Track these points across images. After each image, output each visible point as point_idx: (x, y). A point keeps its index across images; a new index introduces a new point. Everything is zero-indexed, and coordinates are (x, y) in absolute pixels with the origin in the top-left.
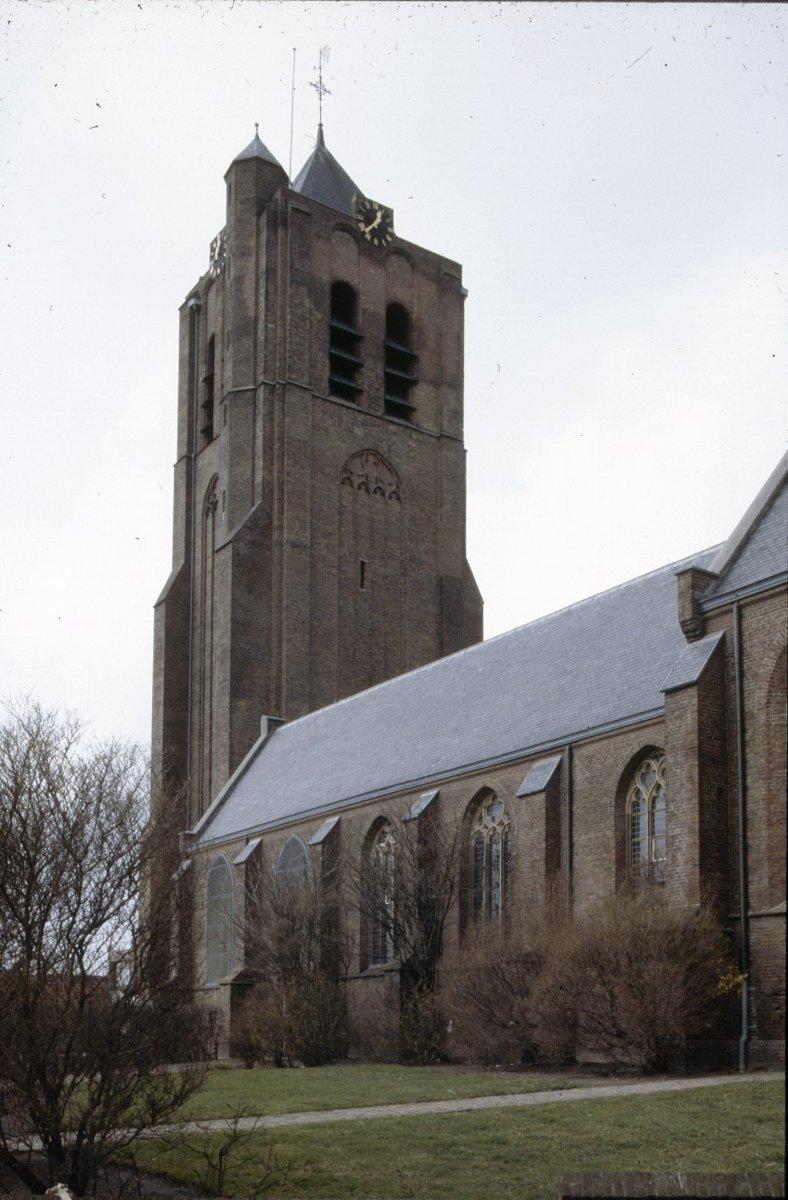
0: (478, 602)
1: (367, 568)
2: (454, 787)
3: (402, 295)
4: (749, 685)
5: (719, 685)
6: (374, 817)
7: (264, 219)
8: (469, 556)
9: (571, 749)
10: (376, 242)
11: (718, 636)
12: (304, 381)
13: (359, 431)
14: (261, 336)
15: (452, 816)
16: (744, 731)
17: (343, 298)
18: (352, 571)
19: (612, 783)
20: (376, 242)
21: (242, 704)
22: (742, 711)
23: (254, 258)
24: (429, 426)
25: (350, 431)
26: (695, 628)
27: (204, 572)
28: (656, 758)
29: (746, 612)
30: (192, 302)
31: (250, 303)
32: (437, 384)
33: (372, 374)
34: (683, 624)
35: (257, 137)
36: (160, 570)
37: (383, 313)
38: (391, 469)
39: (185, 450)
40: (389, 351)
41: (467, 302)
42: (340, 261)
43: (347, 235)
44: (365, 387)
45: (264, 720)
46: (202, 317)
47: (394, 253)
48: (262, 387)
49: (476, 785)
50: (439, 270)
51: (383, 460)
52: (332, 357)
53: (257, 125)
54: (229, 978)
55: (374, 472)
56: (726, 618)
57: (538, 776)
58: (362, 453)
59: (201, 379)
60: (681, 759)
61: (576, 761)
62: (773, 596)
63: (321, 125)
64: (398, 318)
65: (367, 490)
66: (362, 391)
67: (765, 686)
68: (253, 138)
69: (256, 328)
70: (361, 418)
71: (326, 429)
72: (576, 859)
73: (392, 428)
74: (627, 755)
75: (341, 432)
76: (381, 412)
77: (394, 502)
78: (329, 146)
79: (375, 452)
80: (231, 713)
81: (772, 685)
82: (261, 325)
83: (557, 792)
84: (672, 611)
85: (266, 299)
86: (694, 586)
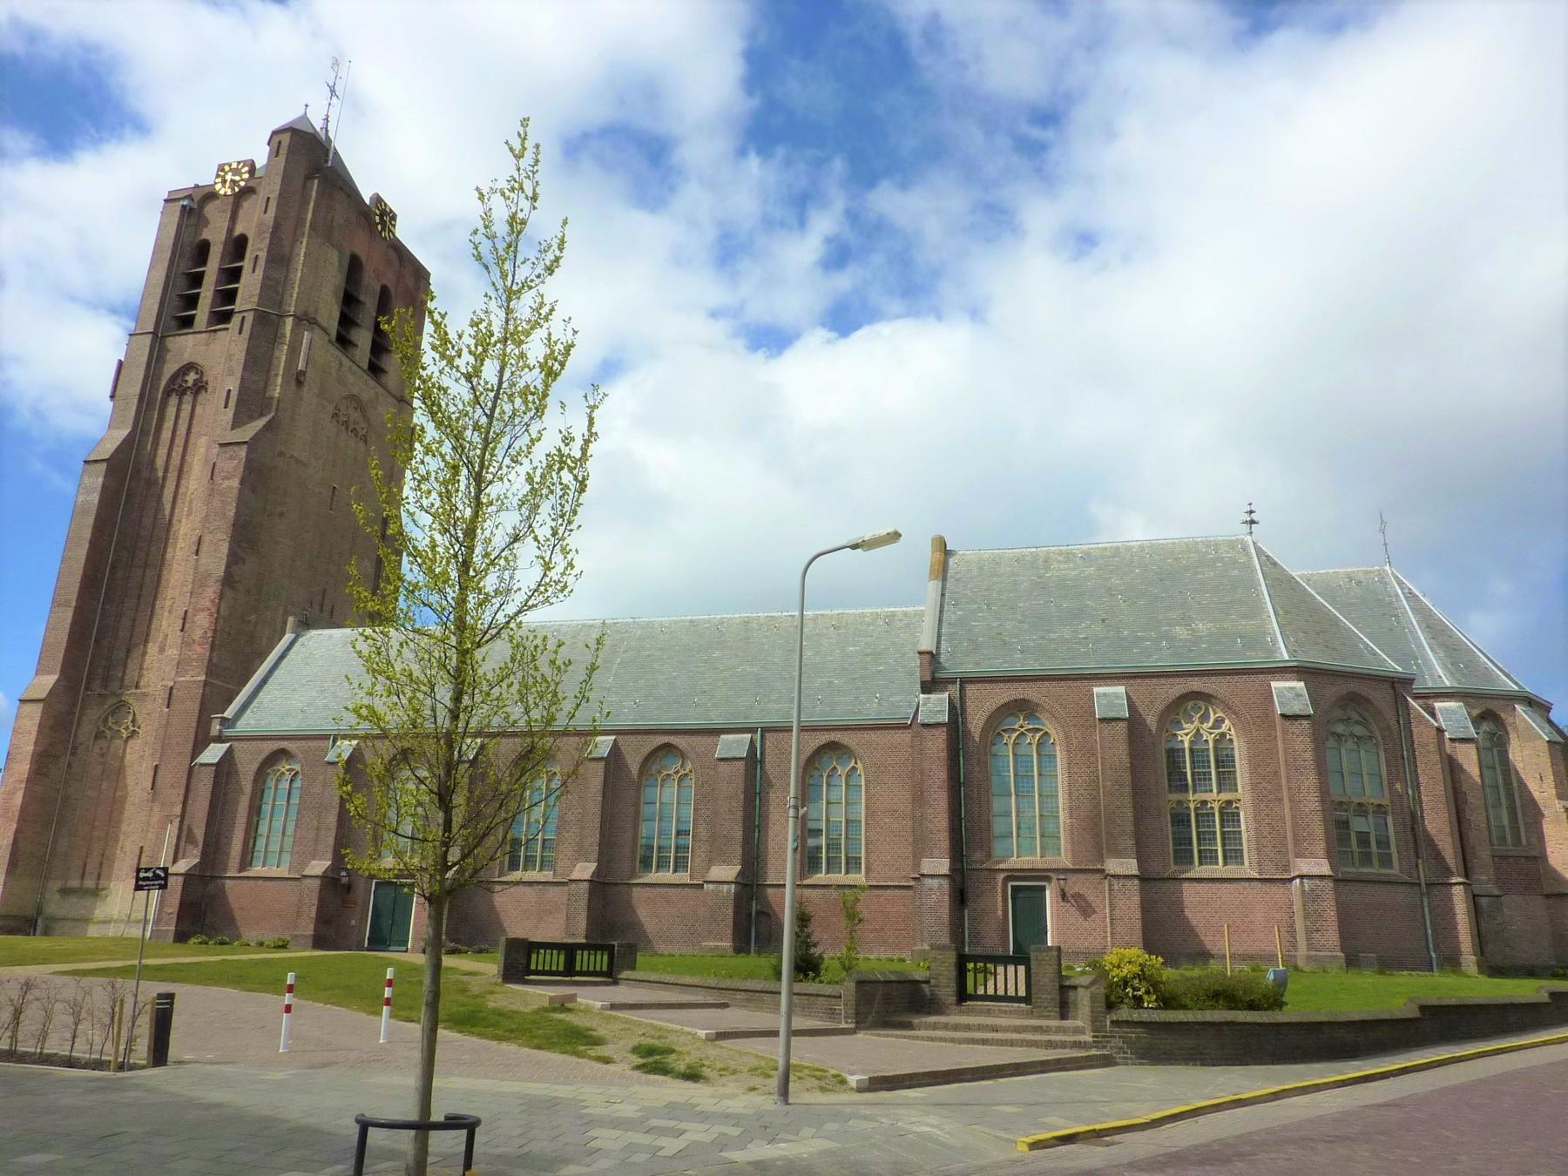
5: (955, 725)
33: (363, 339)
61: (768, 743)
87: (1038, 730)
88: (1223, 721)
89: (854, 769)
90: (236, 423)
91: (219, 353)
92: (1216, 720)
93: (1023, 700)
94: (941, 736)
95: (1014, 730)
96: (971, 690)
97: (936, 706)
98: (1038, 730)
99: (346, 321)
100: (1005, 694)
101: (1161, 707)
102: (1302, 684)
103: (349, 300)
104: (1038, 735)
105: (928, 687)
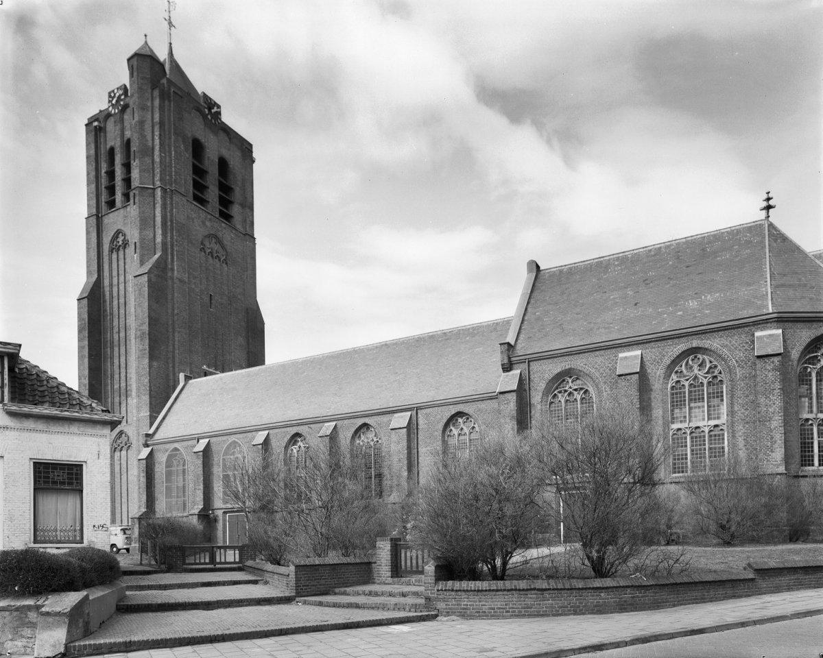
0: (263, 324)
1: (213, 297)
2: (346, 422)
3: (225, 153)
4: (533, 393)
5: (522, 391)
6: (293, 433)
7: (156, 93)
8: (258, 299)
9: (417, 410)
10: (213, 121)
11: (519, 371)
12: (182, 190)
13: (208, 224)
14: (157, 159)
15: (345, 437)
16: (530, 412)
17: (197, 148)
18: (207, 299)
19: (441, 426)
20: (213, 121)
21: (155, 364)
22: (530, 403)
23: (150, 113)
24: (239, 227)
25: (203, 223)
26: (507, 368)
27: (111, 285)
28: (462, 417)
29: (531, 364)
30: (96, 124)
31: (149, 137)
32: (243, 205)
34: (502, 365)
35: (146, 42)
36: (78, 278)
37: (217, 161)
38: (223, 247)
39: (94, 211)
40: (220, 182)
41: (255, 166)
42: (196, 128)
43: (198, 114)
44: (210, 201)
45: (182, 376)
46: (102, 134)
47: (222, 130)
48: (160, 189)
49: (360, 422)
50: (243, 144)
51: (219, 241)
52: (194, 180)
53: (146, 36)
54: (196, 511)
55: (216, 247)
56: (522, 365)
57: (401, 420)
58: (209, 236)
59: (103, 171)
60: (508, 420)
61: (419, 415)
62: (545, 359)
63: (171, 44)
64: (223, 164)
65: (212, 256)
66: (208, 202)
67: (541, 394)
68: (143, 43)
69: (153, 153)
70: (209, 217)
71: (193, 219)
72: (420, 458)
73: (223, 225)
74: (448, 415)
75: (201, 222)
76: (217, 216)
77: (224, 265)
78: (177, 57)
79: (216, 237)
80: (150, 369)
81: (543, 394)
82: (157, 153)
83: (412, 429)
84: (497, 358)
85: (160, 138)
86: (508, 350)
87: (581, 389)
88: (716, 367)
89: (473, 428)
90: (142, 263)
91: (126, 220)
92: (710, 368)
93: (570, 369)
94: (513, 397)
95: (566, 391)
96: (535, 366)
97: (510, 381)
98: (581, 389)
99: (199, 187)
100: (556, 367)
101: (668, 362)
102: (780, 331)
103: (199, 172)
104: (582, 392)
105: (507, 368)
